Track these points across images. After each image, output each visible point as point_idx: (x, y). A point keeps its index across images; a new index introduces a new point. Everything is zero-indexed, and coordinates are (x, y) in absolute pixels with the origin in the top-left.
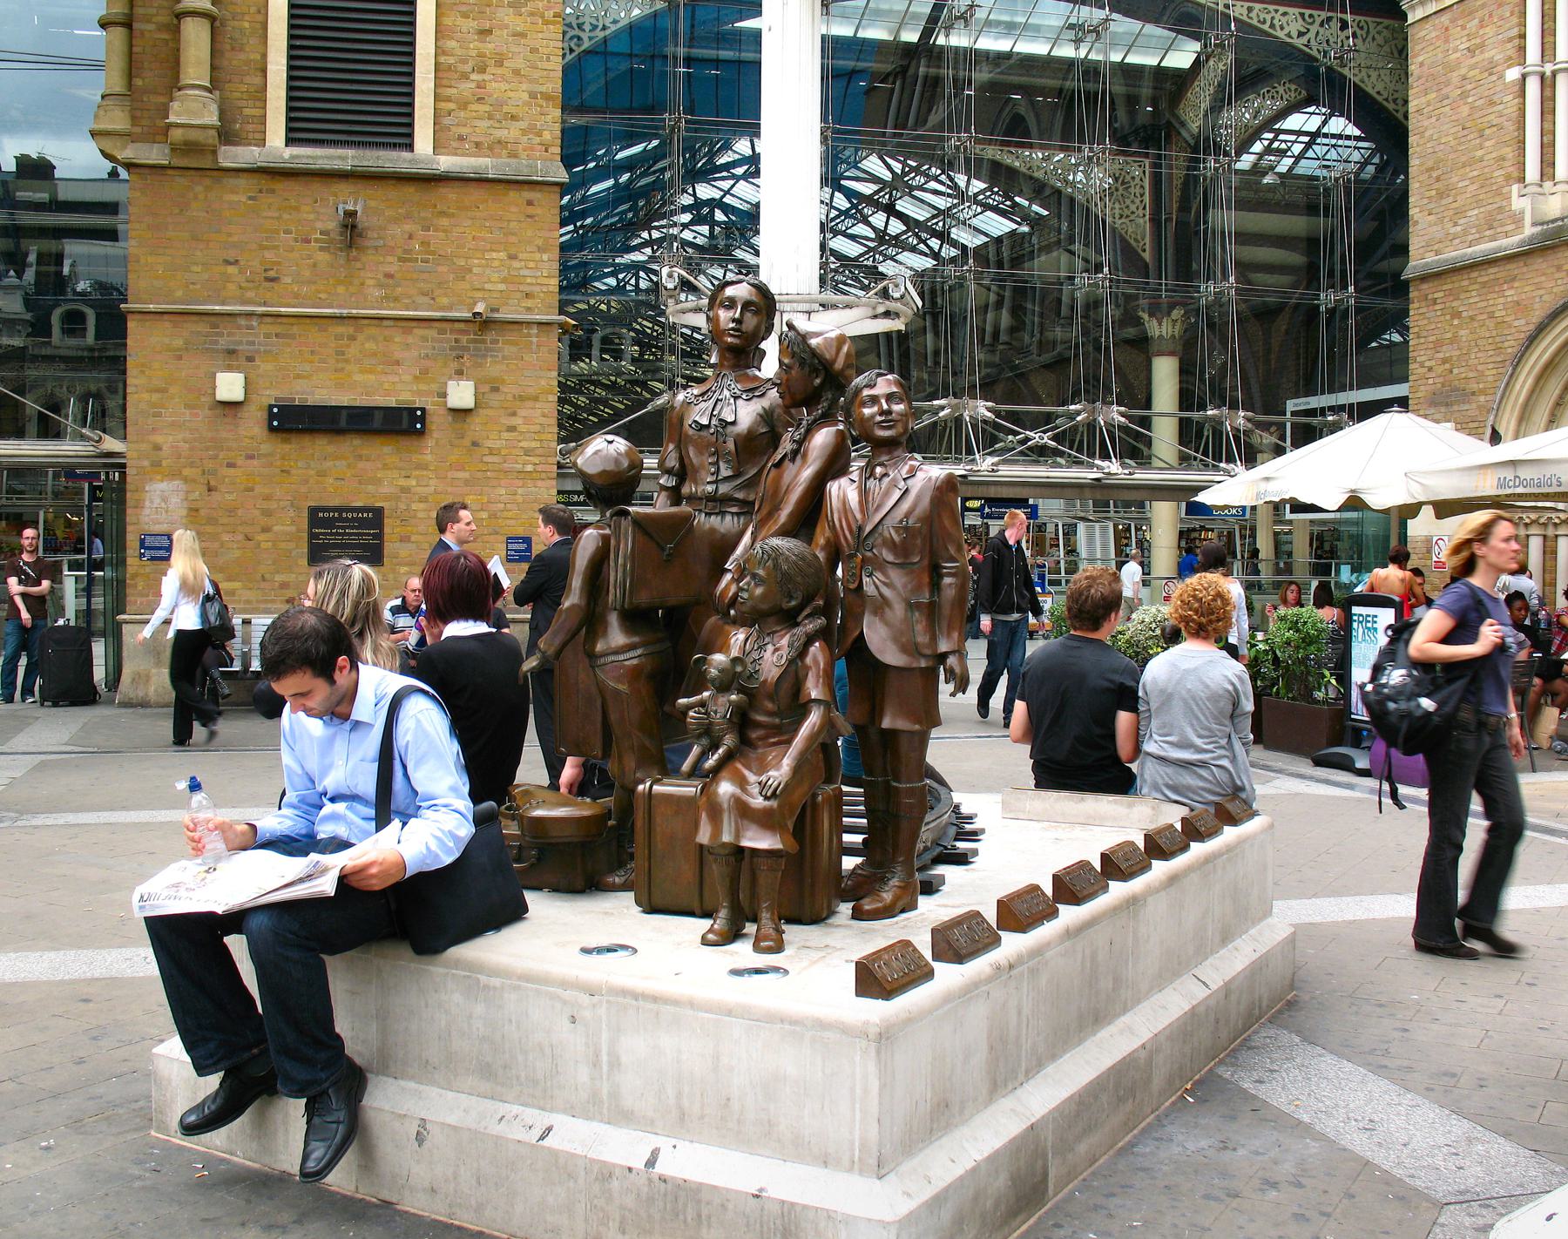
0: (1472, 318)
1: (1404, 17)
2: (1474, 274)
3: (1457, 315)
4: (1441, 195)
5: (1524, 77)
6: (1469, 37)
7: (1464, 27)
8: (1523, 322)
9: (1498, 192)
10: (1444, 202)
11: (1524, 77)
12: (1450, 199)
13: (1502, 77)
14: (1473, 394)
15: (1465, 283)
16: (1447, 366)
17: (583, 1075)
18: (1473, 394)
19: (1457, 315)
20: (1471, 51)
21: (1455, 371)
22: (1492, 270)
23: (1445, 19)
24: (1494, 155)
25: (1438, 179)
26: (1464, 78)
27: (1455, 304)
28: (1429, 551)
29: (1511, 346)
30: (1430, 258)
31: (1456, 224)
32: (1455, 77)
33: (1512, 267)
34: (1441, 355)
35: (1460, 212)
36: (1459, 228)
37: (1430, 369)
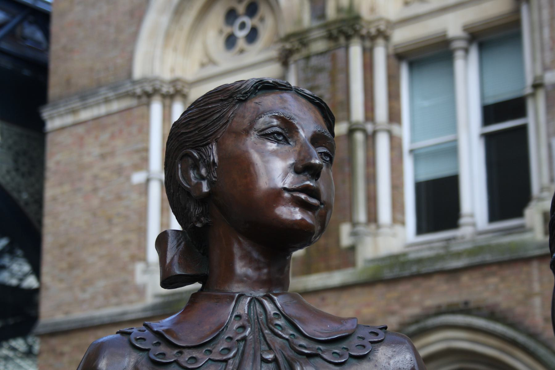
1: (42, 124)
4: (71, 267)
5: (148, 181)
6: (102, 145)
7: (97, 138)
11: (148, 181)
13: (128, 178)
20: (103, 157)
23: (80, 130)
25: (70, 254)
26: (96, 177)
30: (59, 317)
32: (88, 175)
35: (88, 282)
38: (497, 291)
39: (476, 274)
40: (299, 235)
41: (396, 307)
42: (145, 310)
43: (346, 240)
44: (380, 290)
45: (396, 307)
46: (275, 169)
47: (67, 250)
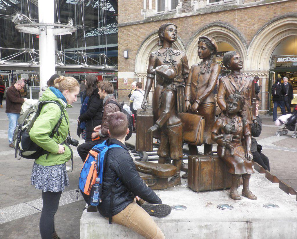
0: (132, 35)
2: (133, 27)
3: (129, 34)
4: (125, 10)
8: (143, 36)
9: (138, 11)
10: (126, 12)
12: (127, 11)
14: (132, 50)
15: (131, 28)
16: (127, 45)
17: (188, 103)
18: (132, 50)
19: (129, 34)
21: (129, 46)
22: (136, 26)
24: (137, 3)
25: (124, 7)
27: (128, 32)
28: (123, 81)
29: (141, 40)
30: (123, 22)
31: (128, 16)
33: (141, 26)
34: (125, 42)
35: (129, 14)
36: (129, 17)
37: (123, 45)
38: (227, 18)
39: (223, 13)
40: (173, 42)
41: (203, 21)
42: (143, 21)
43: (192, 4)
44: (200, 17)
45: (203, 21)
46: (170, 34)
47: (124, 6)
